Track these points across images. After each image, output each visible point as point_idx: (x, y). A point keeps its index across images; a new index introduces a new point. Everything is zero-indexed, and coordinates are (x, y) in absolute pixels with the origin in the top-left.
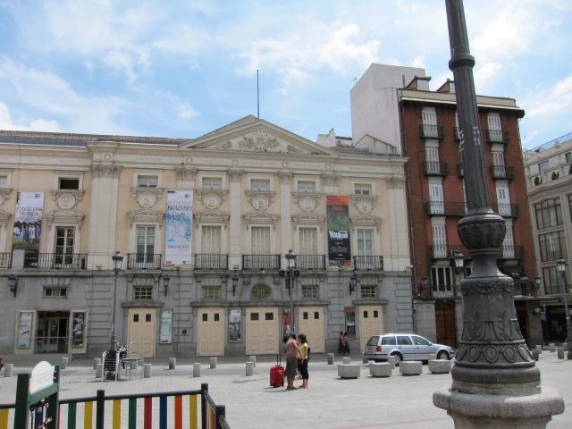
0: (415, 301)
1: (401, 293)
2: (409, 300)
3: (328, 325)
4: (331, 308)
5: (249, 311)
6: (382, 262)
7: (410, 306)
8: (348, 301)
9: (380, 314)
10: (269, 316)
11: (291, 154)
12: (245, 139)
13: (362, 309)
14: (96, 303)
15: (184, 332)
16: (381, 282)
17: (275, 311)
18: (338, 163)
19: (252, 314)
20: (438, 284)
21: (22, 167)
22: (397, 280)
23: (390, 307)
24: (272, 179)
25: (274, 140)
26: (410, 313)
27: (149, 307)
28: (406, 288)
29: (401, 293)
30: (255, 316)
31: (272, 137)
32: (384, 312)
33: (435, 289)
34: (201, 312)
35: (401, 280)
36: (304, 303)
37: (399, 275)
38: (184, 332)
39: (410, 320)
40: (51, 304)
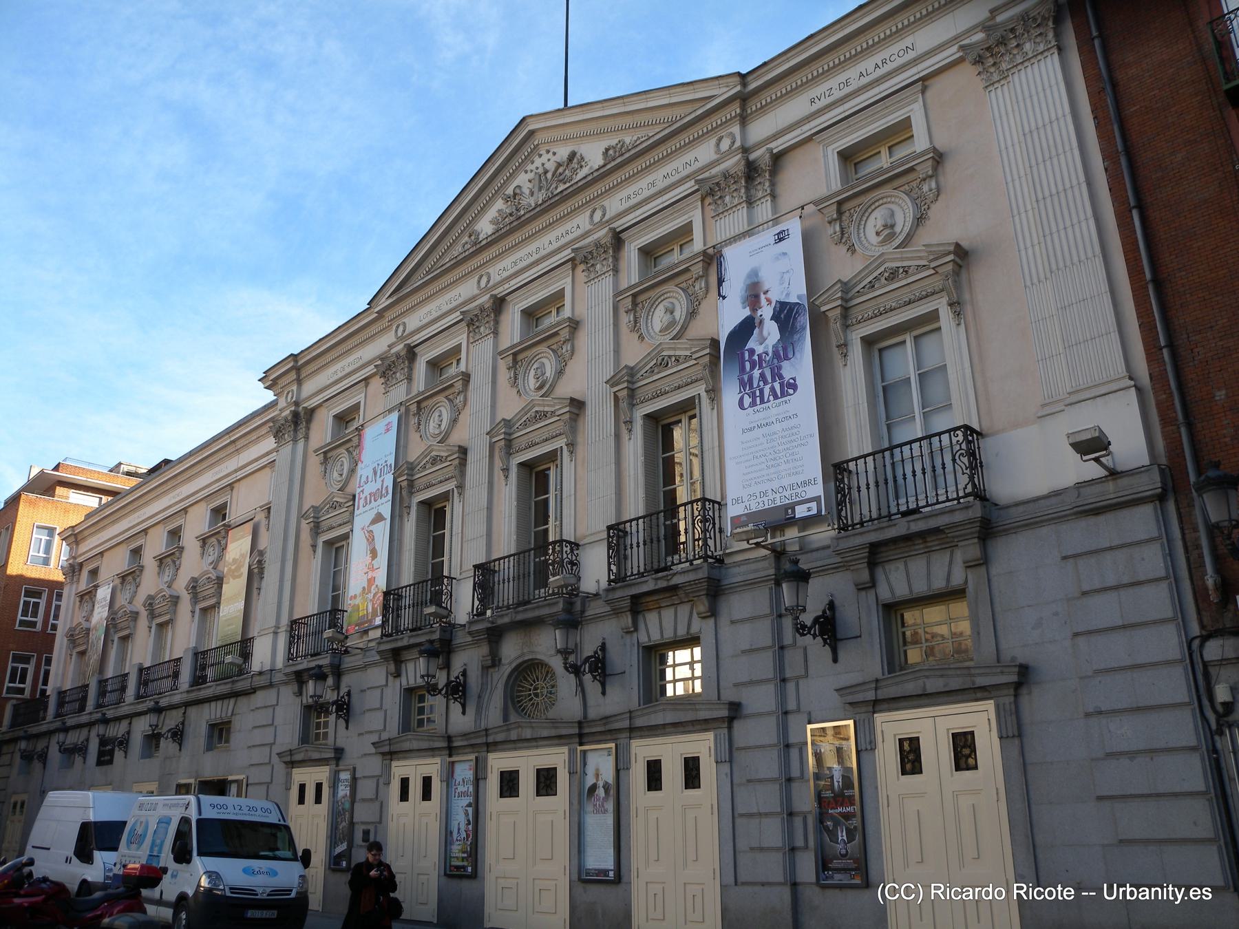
0: (1213, 650)
1: (1105, 610)
2: (1168, 642)
6: (975, 464)
7: (1174, 686)
9: (988, 746)
10: (546, 782)
11: (621, 163)
12: (507, 199)
16: (984, 561)
18: (763, 109)
21: (240, 475)
22: (1078, 535)
23: (1040, 704)
24: (564, 282)
25: (573, 155)
26: (1182, 728)
29: (1105, 610)
31: (563, 152)
32: (1013, 731)
35: (1107, 530)
36: (639, 722)
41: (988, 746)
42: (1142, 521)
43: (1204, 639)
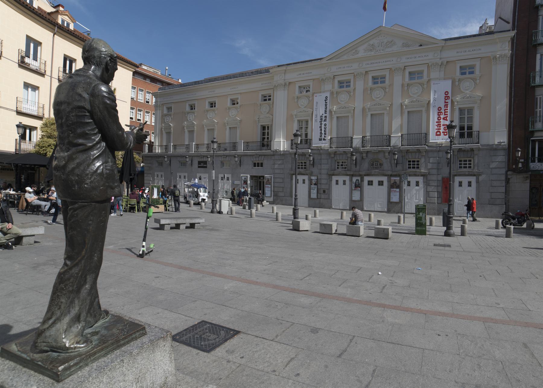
0: (509, 173)
2: (503, 171)
3: (427, 191)
4: (429, 177)
5: (367, 179)
7: (503, 178)
8: (445, 172)
10: (381, 183)
13: (457, 179)
14: (277, 171)
15: (324, 191)
17: (385, 179)
19: (369, 181)
20: (530, 156)
27: (304, 175)
28: (501, 158)
30: (370, 183)
32: (478, 182)
33: (533, 161)
34: (334, 178)
37: (493, 149)
38: (324, 191)
39: (503, 189)
40: (257, 171)
41: (474, 184)
42: (502, 153)
43: (507, 171)
